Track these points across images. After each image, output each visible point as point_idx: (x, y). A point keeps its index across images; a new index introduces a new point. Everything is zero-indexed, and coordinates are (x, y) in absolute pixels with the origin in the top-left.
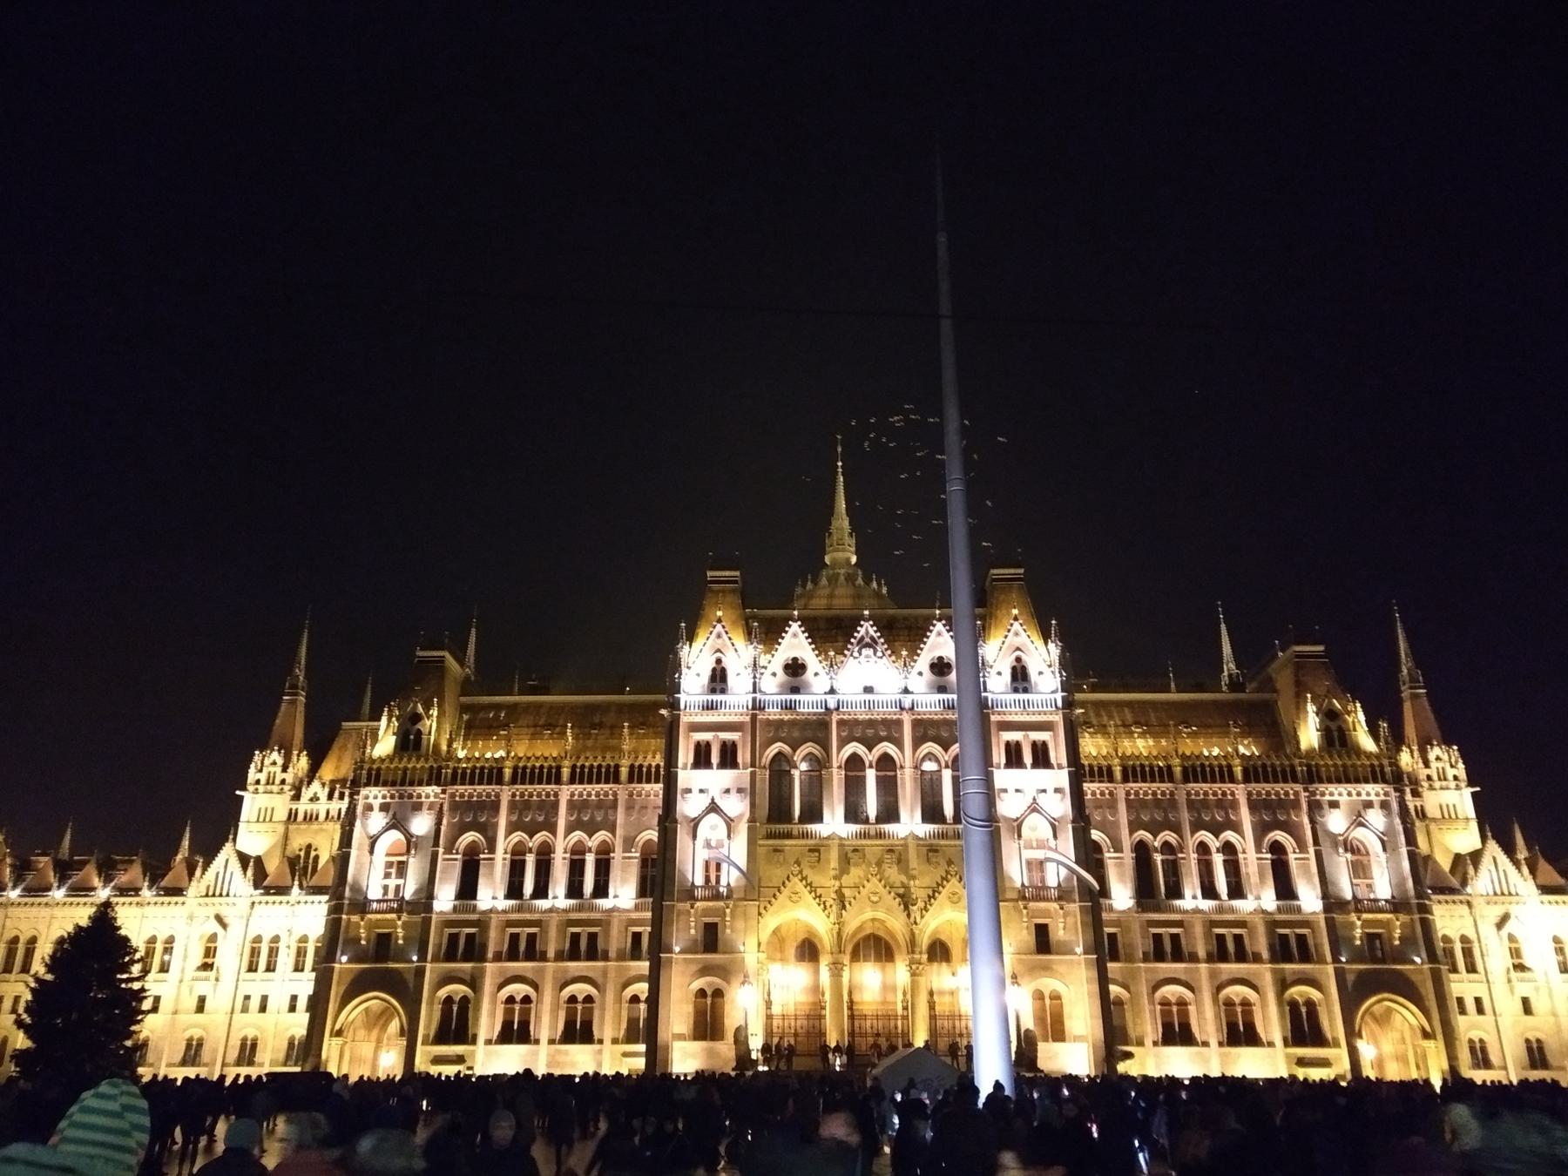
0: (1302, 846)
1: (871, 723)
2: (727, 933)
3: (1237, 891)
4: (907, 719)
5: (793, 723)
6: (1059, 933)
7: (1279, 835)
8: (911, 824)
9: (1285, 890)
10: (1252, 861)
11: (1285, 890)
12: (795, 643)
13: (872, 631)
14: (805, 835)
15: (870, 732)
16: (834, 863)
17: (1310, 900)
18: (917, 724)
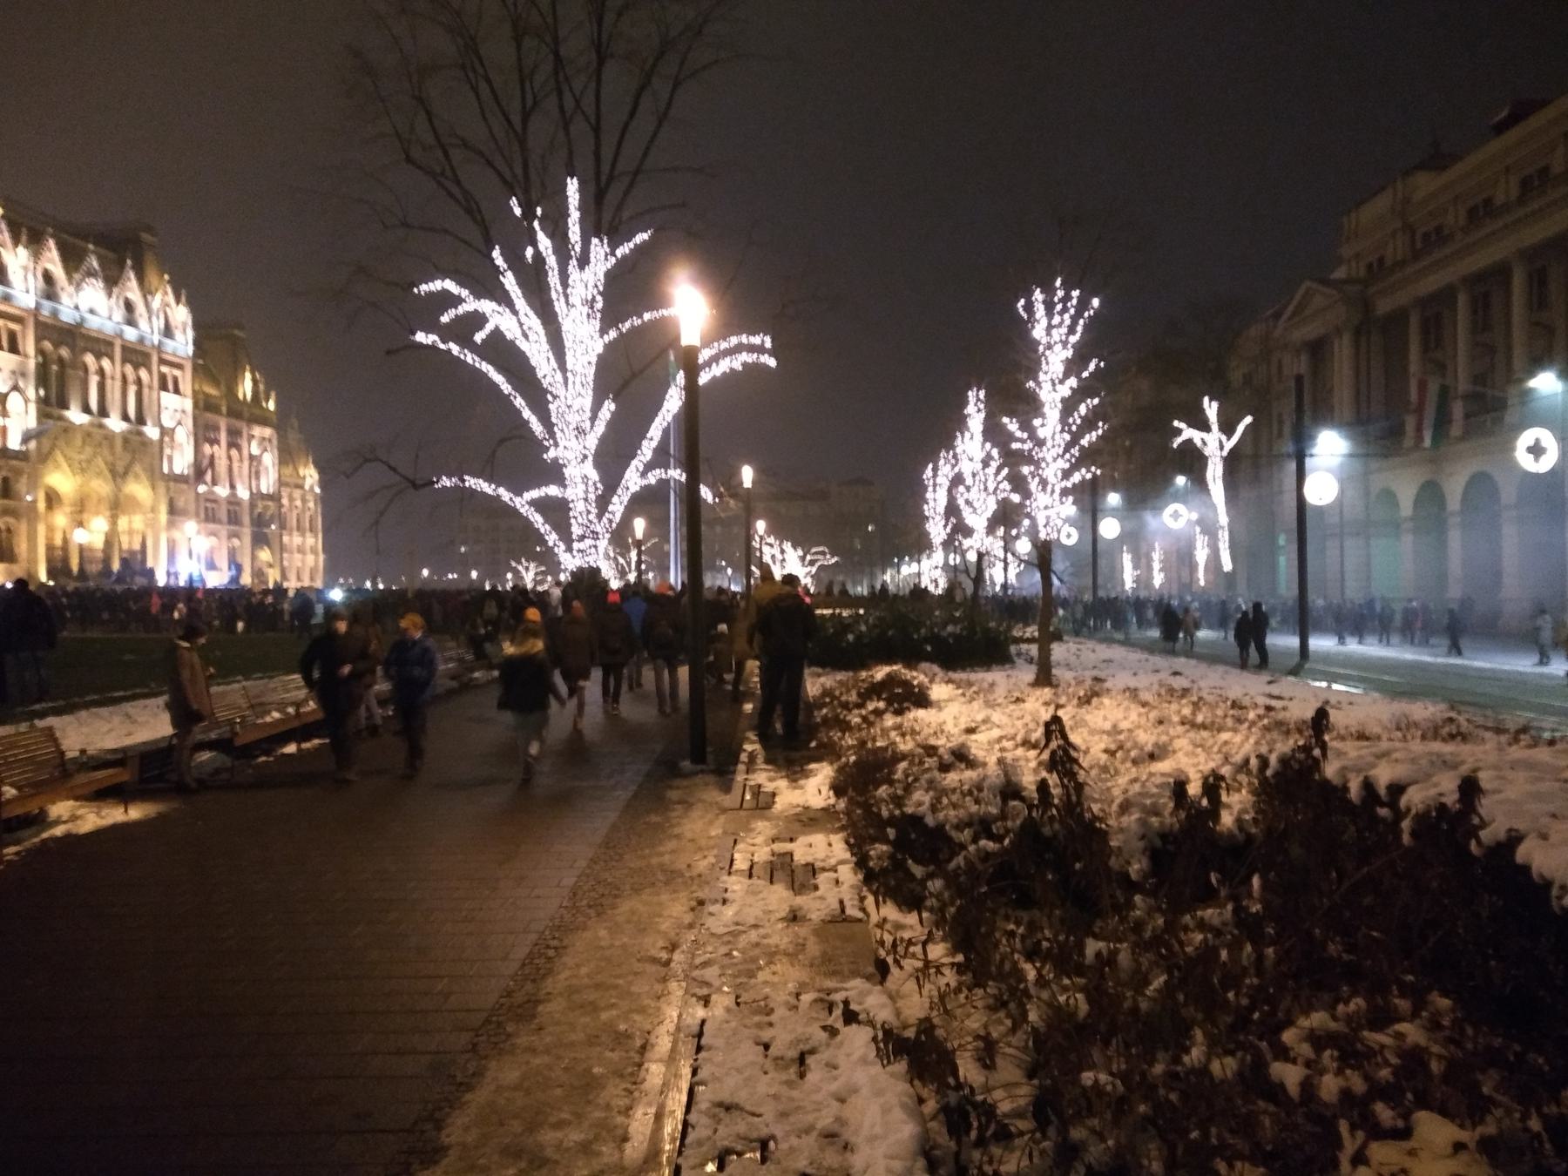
0: (241, 460)
1: (97, 340)
2: (21, 485)
3: (214, 483)
4: (118, 343)
5: (53, 327)
6: (180, 503)
7: (234, 452)
8: (115, 424)
9: (233, 487)
10: (222, 465)
11: (233, 487)
12: (52, 260)
13: (95, 264)
14: (61, 418)
15: (96, 347)
16: (79, 442)
17: (243, 493)
18: (125, 348)
